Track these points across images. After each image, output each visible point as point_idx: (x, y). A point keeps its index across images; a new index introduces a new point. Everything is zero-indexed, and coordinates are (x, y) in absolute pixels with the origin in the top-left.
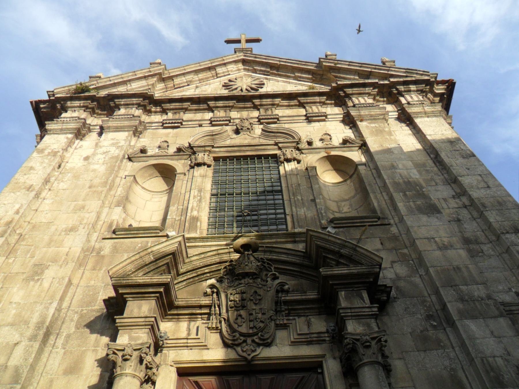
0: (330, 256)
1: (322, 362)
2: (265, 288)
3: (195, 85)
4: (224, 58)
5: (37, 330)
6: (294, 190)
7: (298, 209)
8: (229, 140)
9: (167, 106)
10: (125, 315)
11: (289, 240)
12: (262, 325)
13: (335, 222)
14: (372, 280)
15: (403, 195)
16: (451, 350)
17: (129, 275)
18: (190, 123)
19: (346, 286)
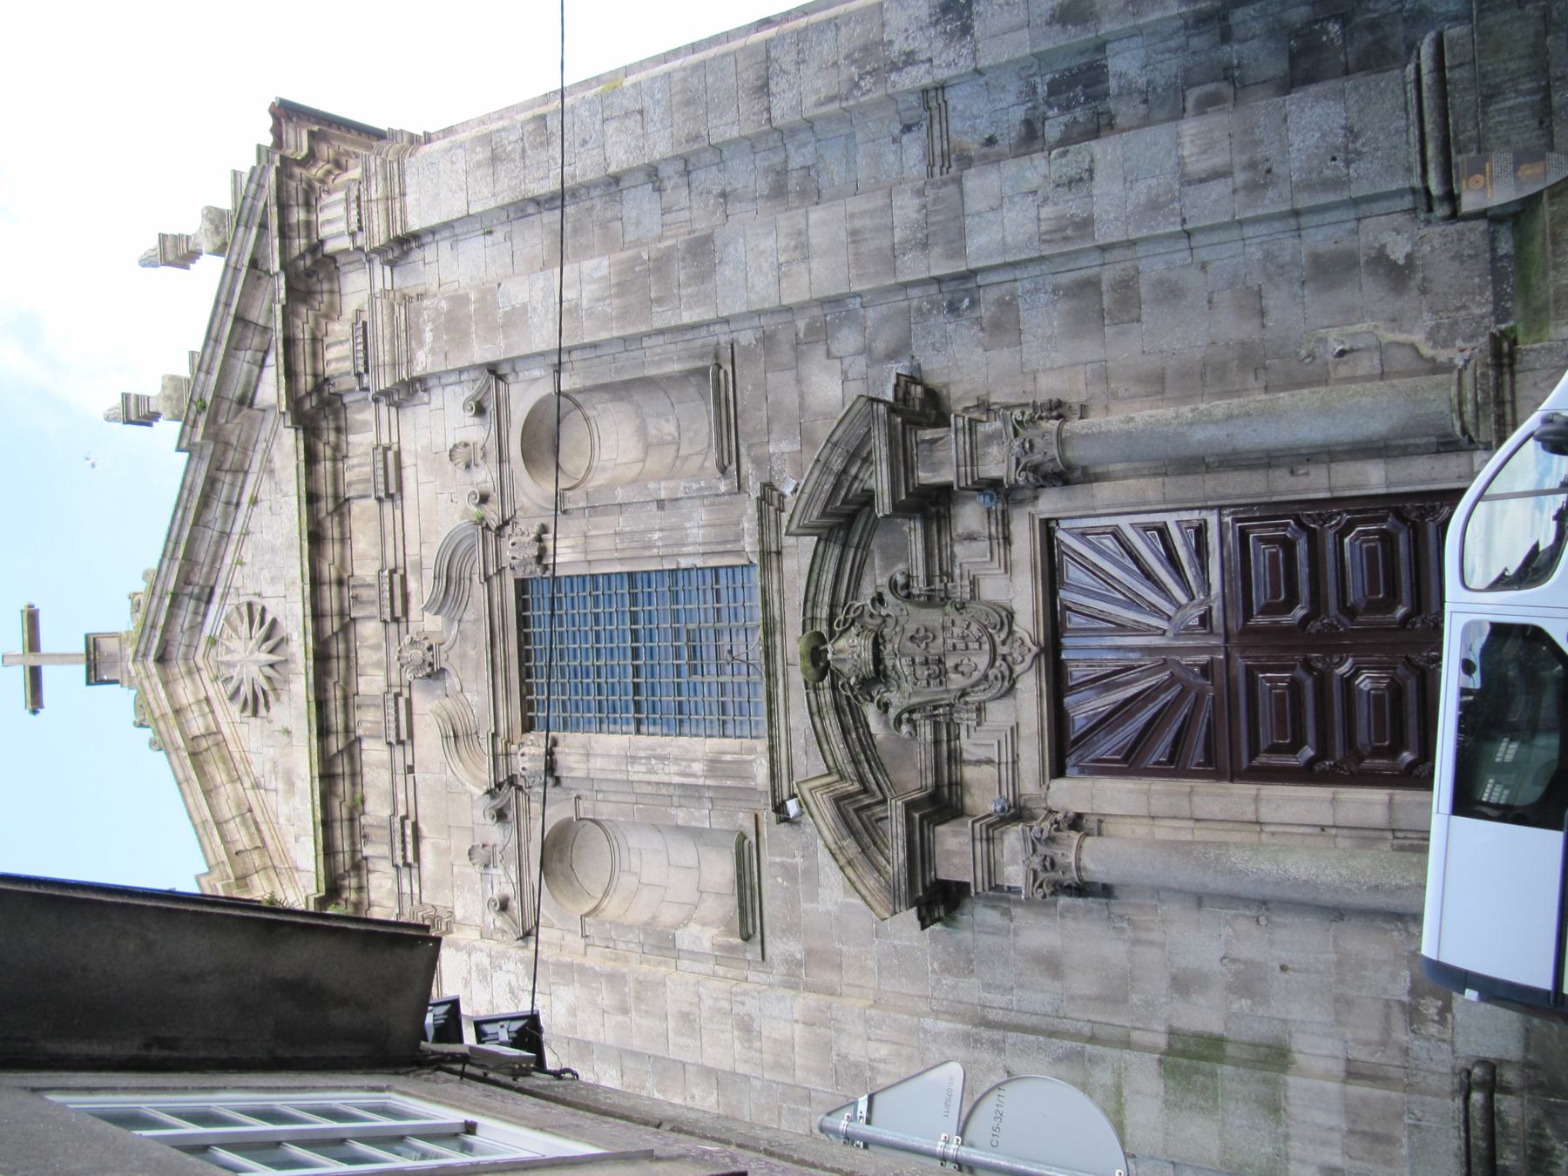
0: (843, 493)
1: (1041, 520)
2: (902, 620)
3: (250, 793)
4: (157, 714)
5: (982, 1044)
6: (633, 545)
7: (690, 540)
8: (469, 696)
9: (343, 860)
10: (968, 879)
11: (774, 564)
12: (974, 628)
13: (726, 462)
14: (899, 420)
15: (661, 306)
16: (1018, 284)
17: (887, 882)
18: (401, 797)
19: (910, 469)
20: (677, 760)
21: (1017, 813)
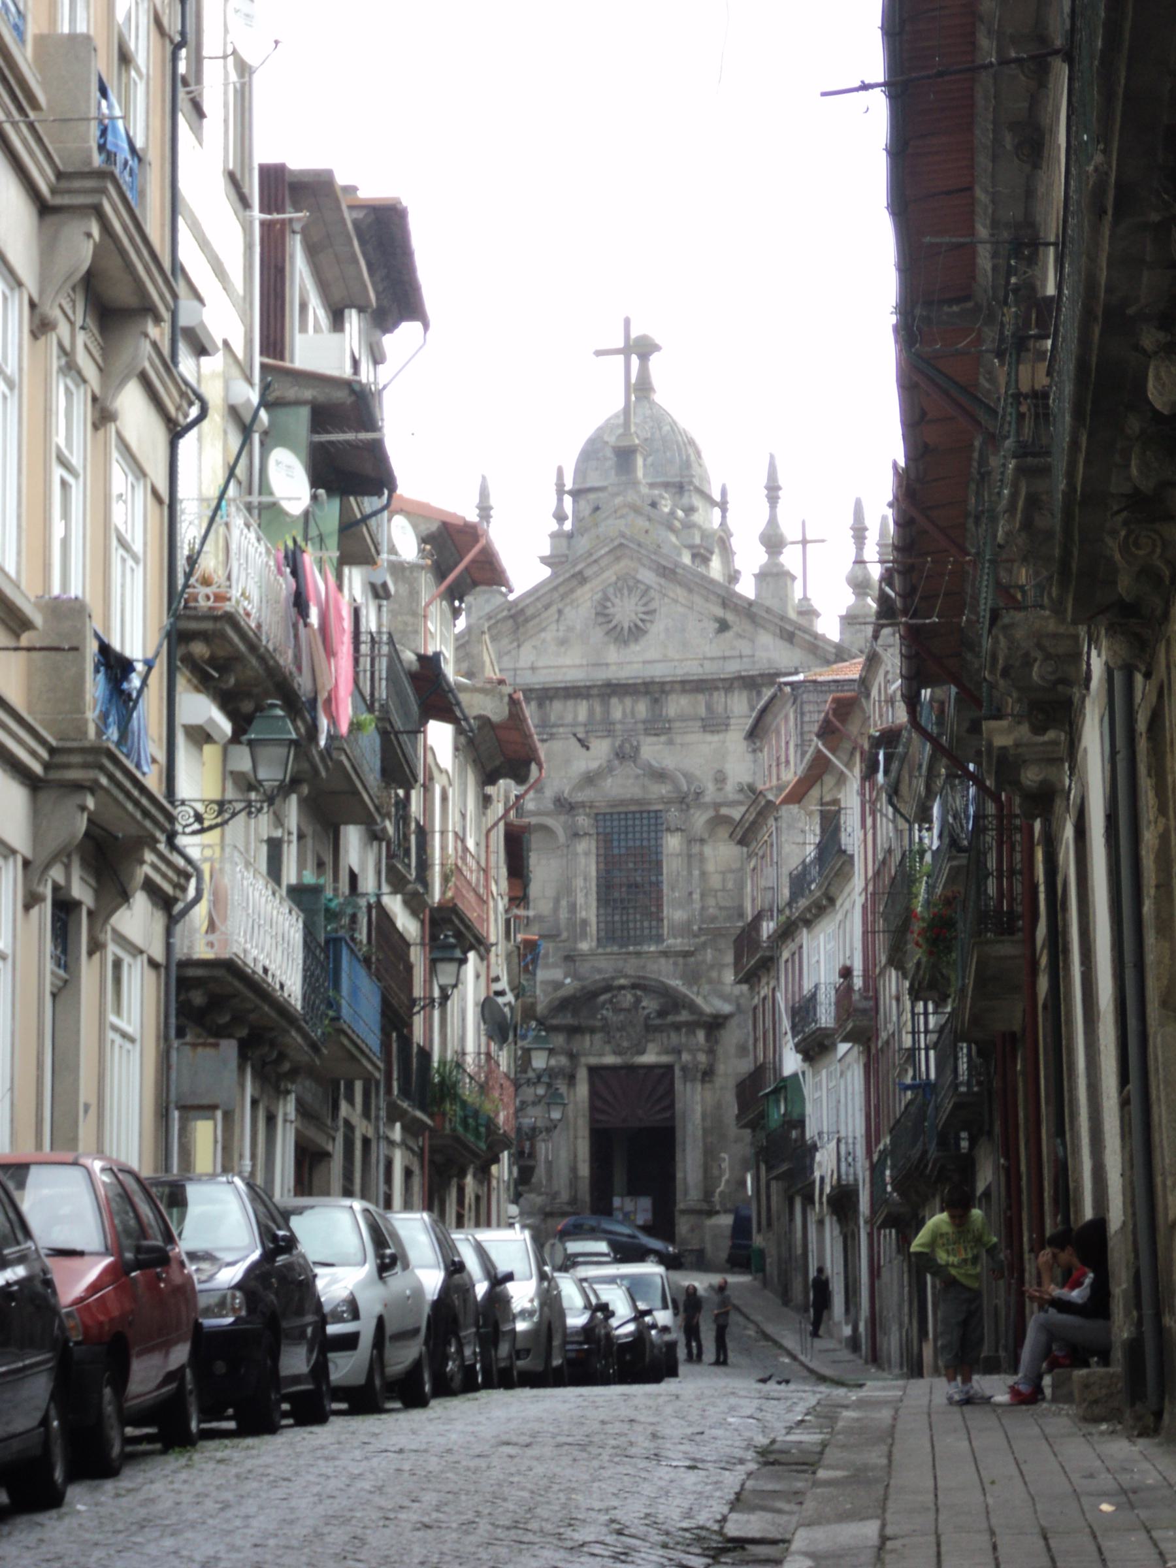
8: (609, 780)
18: (561, 730)
20: (586, 903)
21: (573, 1057)
